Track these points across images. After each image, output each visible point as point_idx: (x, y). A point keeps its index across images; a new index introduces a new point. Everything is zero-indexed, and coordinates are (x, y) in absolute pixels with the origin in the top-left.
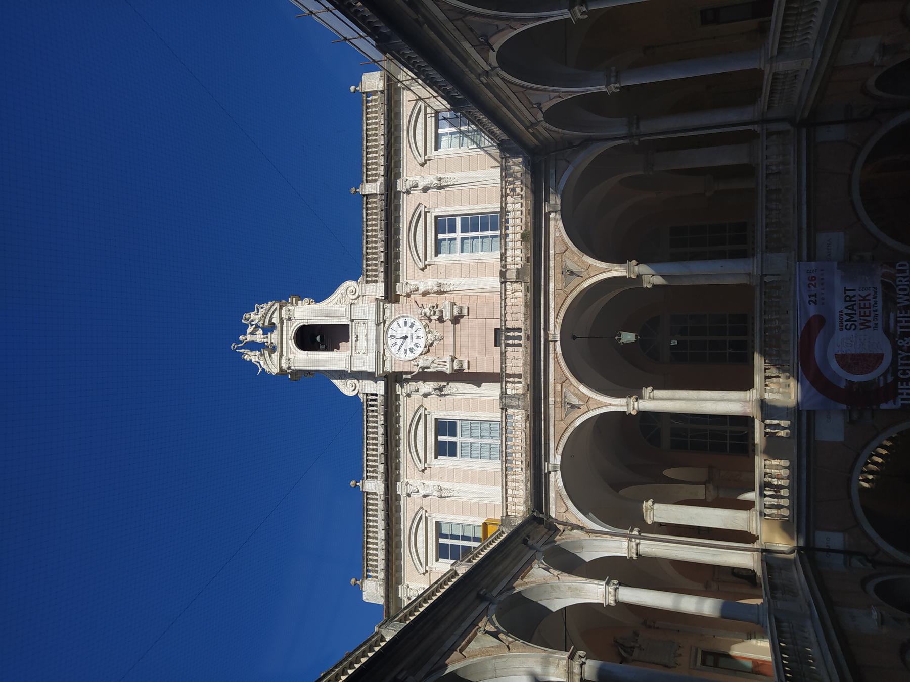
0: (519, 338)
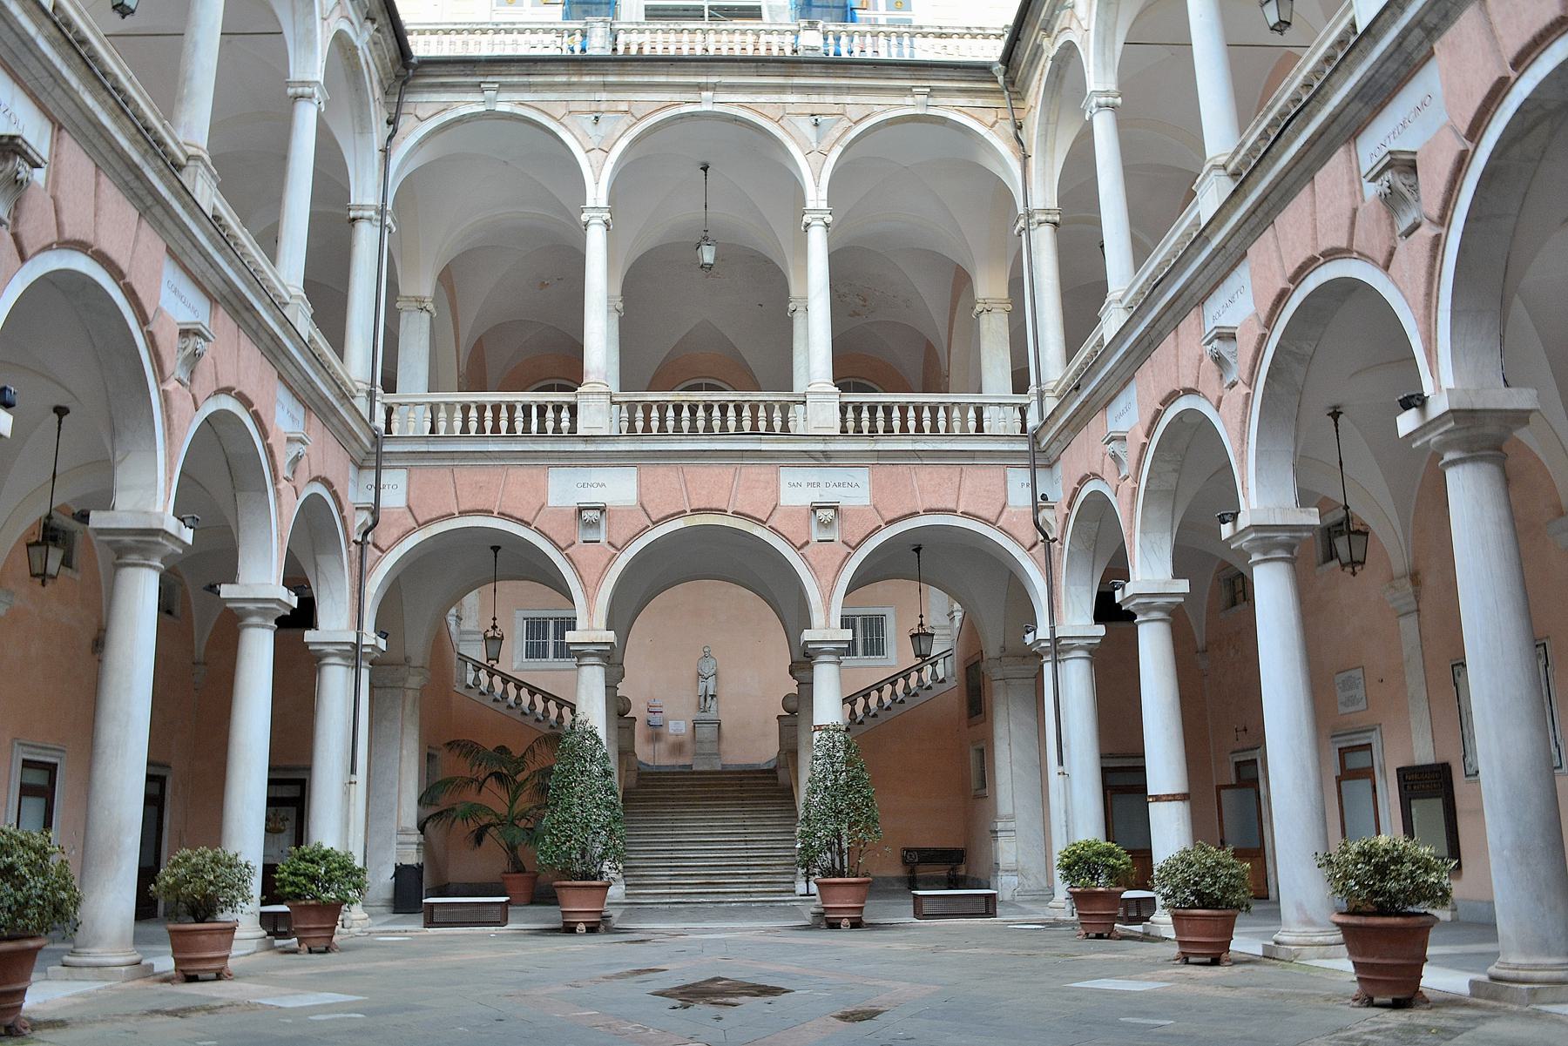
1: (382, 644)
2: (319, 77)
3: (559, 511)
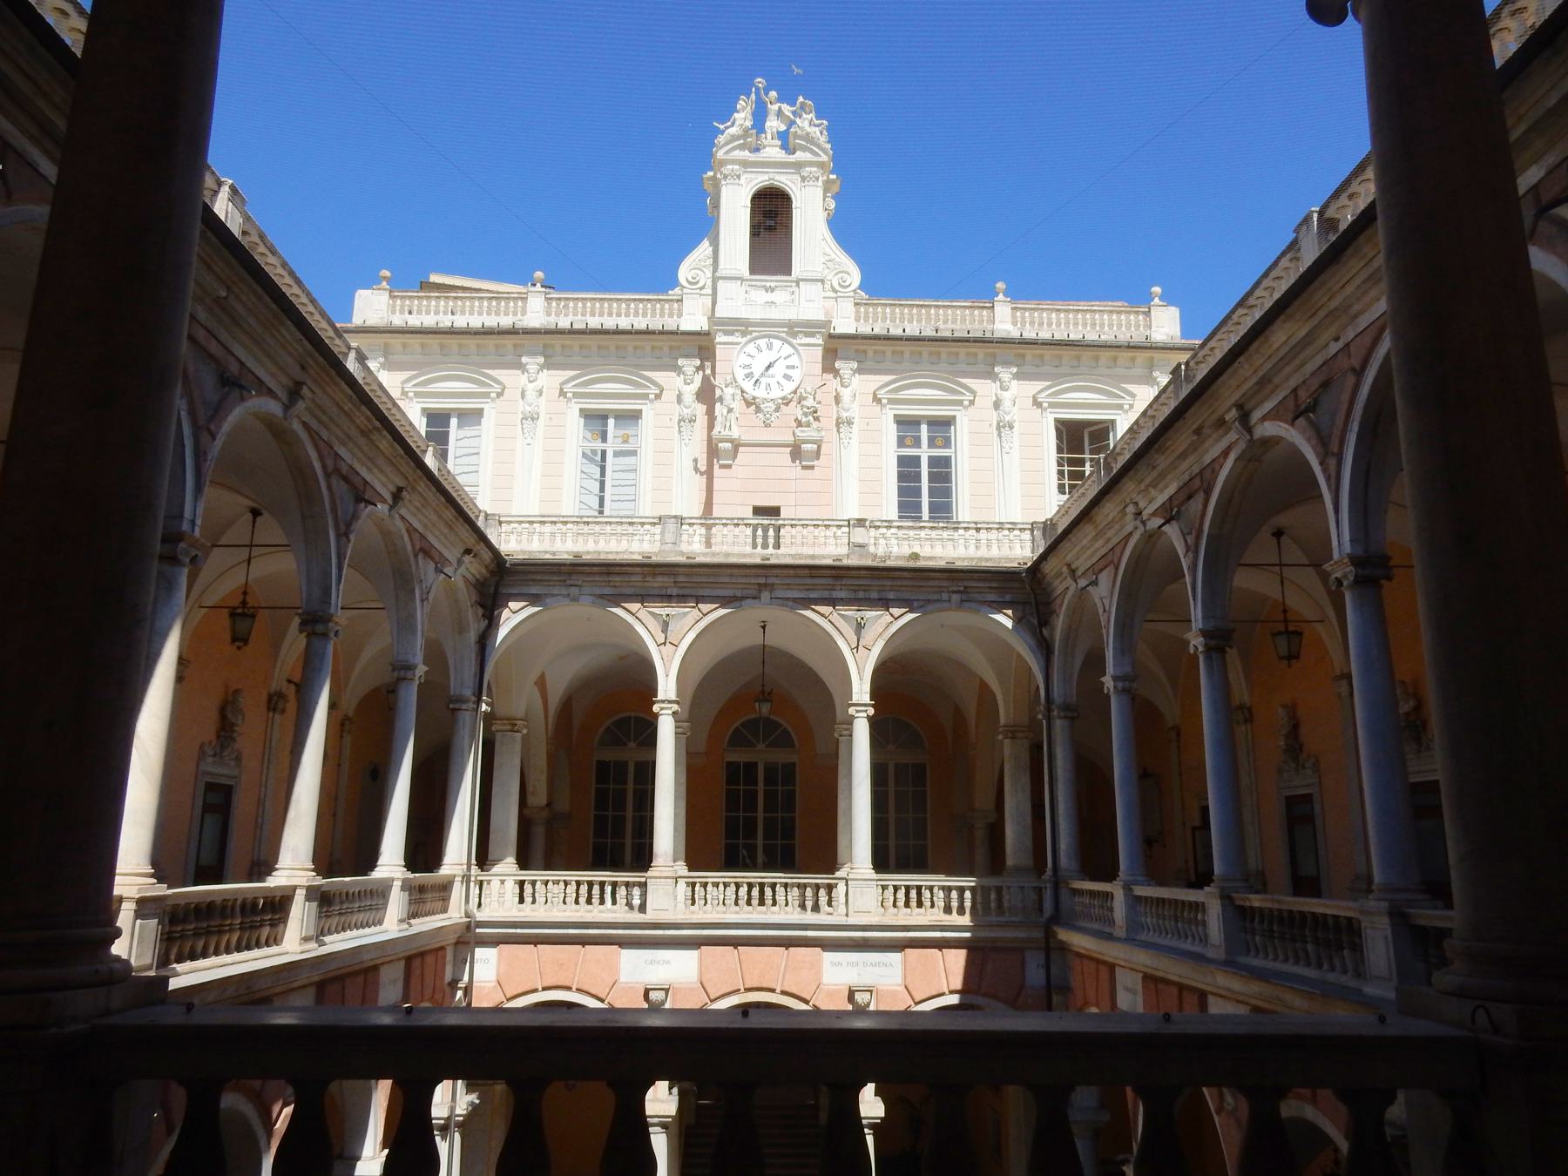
0: (765, 546)
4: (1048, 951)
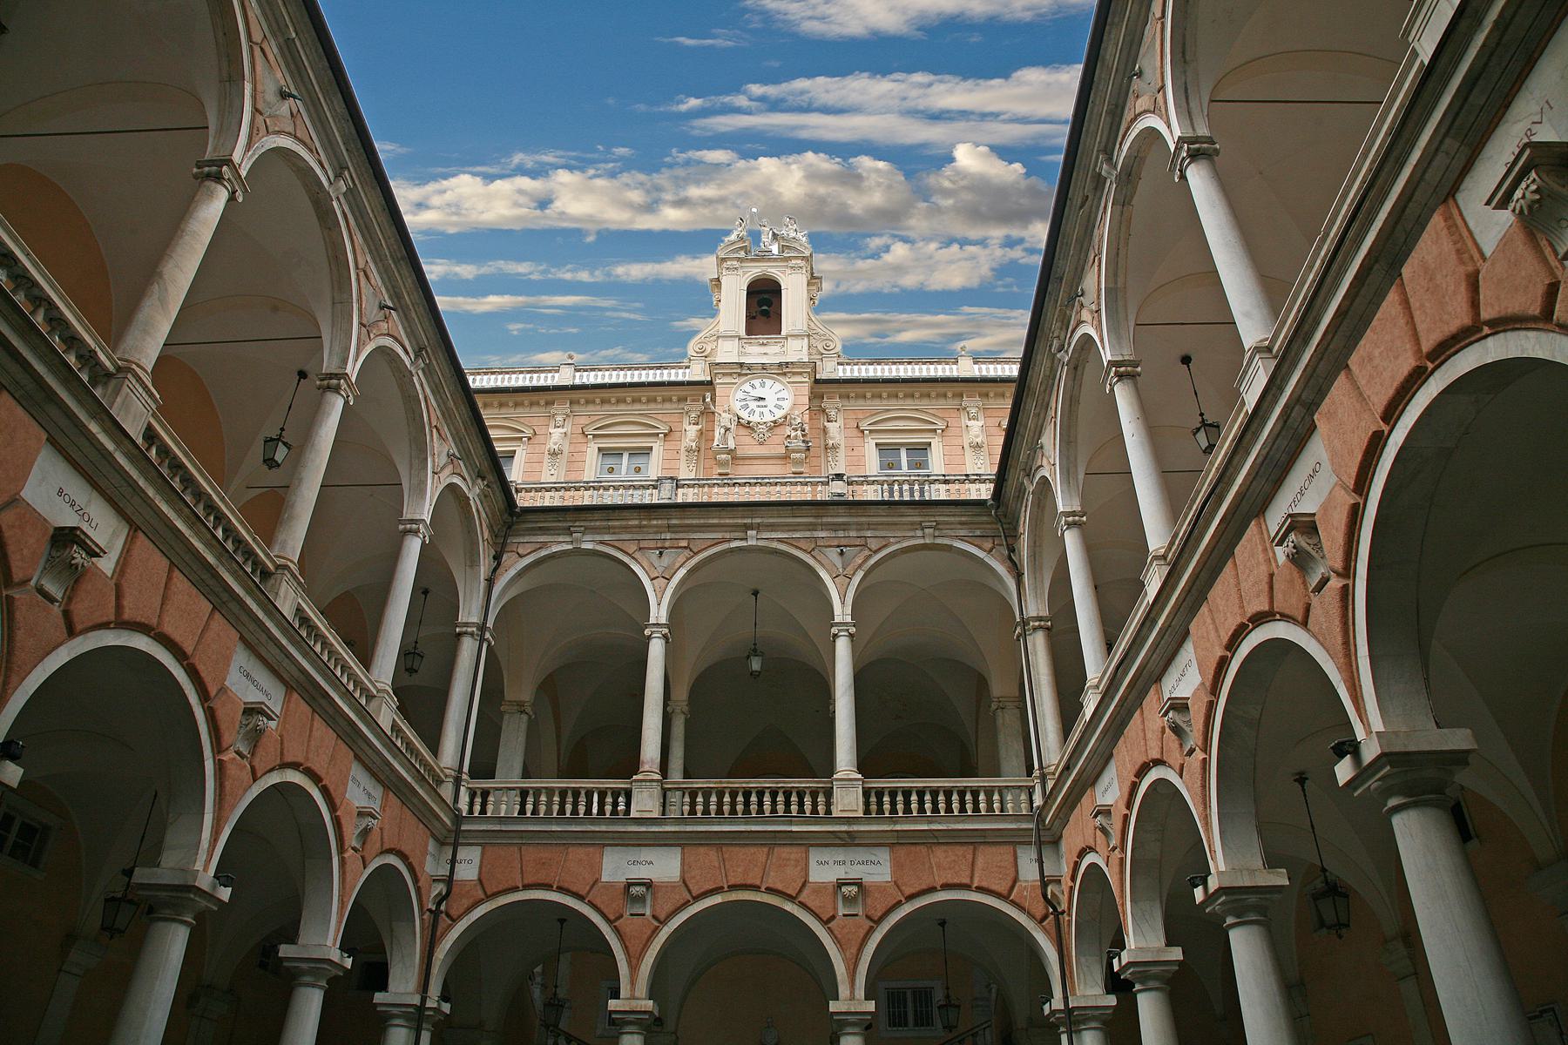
1: (446, 1008)
2: (427, 518)
3: (611, 885)
4: (1040, 845)
